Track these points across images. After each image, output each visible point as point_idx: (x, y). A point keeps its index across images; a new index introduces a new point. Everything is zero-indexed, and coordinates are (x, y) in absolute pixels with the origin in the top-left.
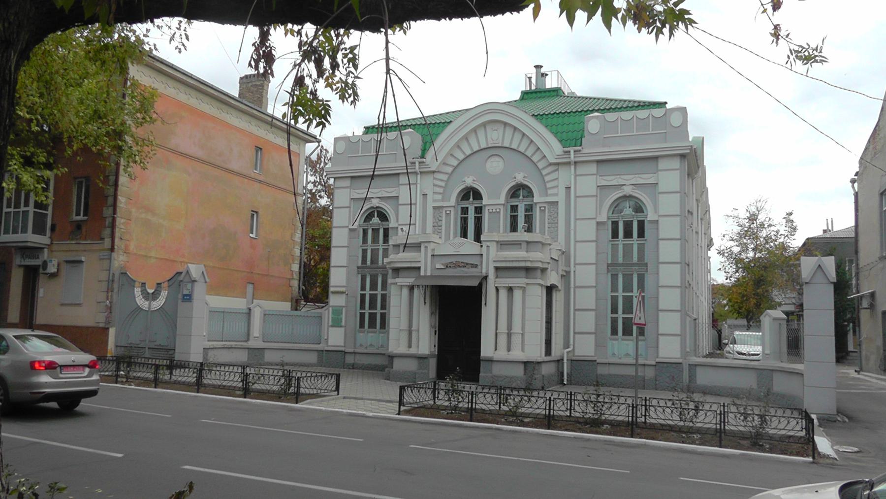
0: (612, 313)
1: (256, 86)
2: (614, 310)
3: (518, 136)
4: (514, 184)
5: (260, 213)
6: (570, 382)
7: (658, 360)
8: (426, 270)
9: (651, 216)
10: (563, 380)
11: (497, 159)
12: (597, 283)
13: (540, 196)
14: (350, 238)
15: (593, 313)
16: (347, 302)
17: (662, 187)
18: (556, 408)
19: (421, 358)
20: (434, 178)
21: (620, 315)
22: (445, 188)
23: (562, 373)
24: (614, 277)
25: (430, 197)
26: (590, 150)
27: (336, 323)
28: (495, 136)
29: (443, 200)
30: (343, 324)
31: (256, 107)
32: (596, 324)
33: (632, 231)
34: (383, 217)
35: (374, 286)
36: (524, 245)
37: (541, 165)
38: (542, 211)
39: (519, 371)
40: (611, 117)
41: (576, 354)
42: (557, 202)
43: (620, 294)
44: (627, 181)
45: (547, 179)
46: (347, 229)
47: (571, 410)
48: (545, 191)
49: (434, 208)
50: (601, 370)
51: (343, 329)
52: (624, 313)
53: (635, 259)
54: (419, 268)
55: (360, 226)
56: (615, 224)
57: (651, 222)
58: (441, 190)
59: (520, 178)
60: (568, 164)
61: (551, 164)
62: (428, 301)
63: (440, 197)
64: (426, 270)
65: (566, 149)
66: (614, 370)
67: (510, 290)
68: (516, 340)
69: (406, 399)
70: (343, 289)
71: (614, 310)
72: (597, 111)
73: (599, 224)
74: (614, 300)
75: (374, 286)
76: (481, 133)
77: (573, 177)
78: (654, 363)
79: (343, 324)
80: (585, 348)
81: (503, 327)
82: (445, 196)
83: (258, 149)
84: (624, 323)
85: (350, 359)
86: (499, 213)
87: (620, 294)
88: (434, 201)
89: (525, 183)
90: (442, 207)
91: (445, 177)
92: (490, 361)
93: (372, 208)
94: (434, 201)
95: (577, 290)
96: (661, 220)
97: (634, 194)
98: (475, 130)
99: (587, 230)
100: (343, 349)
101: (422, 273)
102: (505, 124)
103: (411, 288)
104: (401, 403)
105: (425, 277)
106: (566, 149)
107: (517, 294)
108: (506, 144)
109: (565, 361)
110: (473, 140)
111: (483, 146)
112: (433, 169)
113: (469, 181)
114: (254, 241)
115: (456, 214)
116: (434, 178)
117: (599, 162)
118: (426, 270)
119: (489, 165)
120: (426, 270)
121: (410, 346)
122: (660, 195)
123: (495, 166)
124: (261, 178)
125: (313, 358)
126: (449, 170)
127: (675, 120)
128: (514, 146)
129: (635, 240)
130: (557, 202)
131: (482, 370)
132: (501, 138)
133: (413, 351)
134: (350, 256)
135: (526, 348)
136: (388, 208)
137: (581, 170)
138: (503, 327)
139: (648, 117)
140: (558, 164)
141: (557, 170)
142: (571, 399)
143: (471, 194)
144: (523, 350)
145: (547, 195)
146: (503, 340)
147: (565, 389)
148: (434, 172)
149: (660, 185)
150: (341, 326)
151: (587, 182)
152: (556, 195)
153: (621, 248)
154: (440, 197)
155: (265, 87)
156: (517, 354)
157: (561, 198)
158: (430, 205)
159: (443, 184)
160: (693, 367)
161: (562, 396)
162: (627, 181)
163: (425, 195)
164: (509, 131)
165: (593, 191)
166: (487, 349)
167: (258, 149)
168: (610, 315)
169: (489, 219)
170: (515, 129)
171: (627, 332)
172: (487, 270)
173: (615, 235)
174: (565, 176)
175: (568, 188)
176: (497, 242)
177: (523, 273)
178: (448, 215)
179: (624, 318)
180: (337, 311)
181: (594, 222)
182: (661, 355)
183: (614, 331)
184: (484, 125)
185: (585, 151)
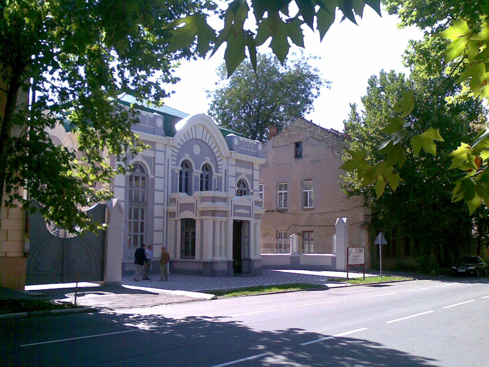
19: (228, 262)
34: (143, 170)
35: (136, 217)
42: (221, 177)
45: (219, 163)
59: (208, 160)
63: (175, 163)
75: (136, 217)
88: (173, 165)
93: (137, 161)
94: (173, 165)
103: (221, 222)
113: (187, 156)
116: (172, 151)
117: (236, 160)
133: (224, 258)
145: (218, 172)
152: (221, 173)
158: (171, 167)
159: (176, 155)
163: (168, 160)
165: (234, 175)
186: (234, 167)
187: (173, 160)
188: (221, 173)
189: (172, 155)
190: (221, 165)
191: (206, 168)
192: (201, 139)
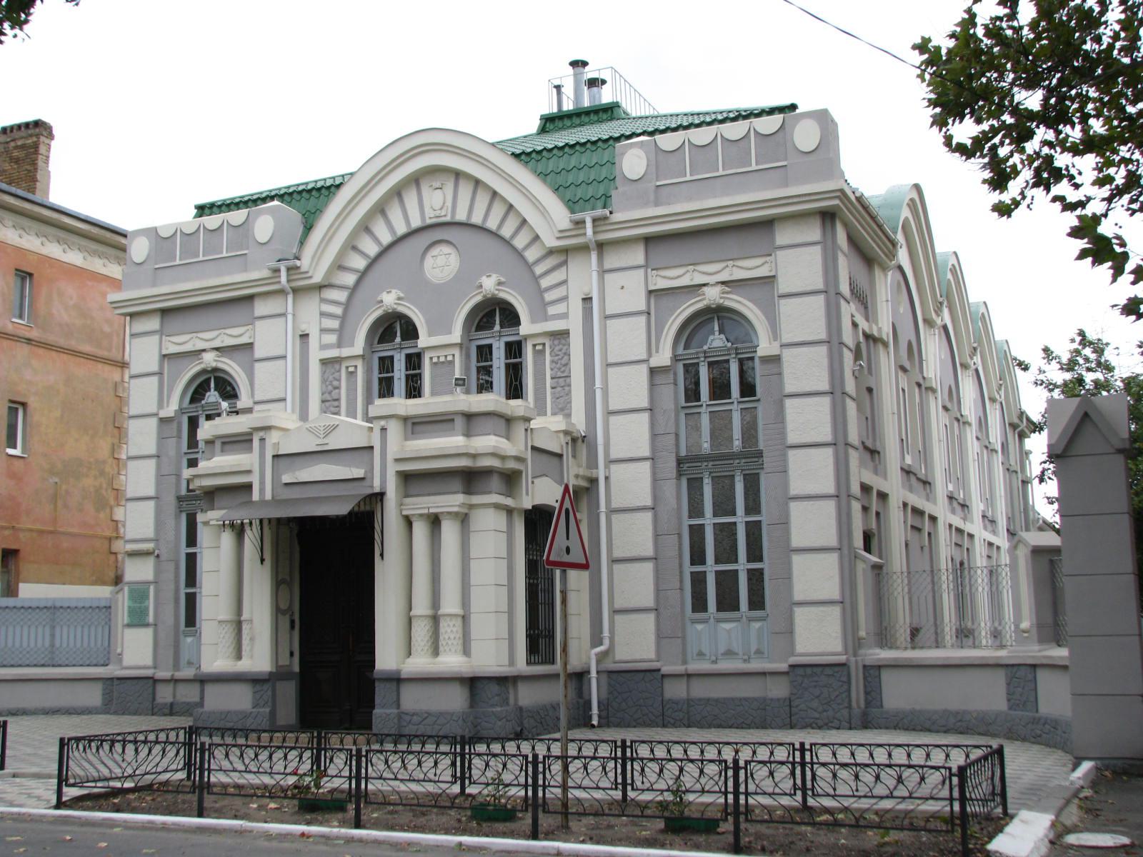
0: (761, 572)
1: (23, 147)
2: (698, 556)
3: (482, 200)
4: (479, 298)
5: (33, 402)
6: (605, 722)
7: (793, 660)
8: (262, 490)
9: (765, 346)
10: (590, 718)
11: (445, 249)
12: (655, 497)
13: (534, 321)
14: (161, 438)
15: (649, 566)
16: (158, 571)
17: (783, 286)
18: (752, 788)
19: (255, 680)
20: (323, 300)
21: (711, 568)
22: (343, 318)
23: (589, 703)
24: (695, 486)
25: (313, 342)
26: (629, 214)
27: (138, 619)
28: (436, 202)
29: (339, 345)
30: (151, 619)
31: (20, 192)
32: (658, 591)
33: (728, 385)
36: (459, 422)
37: (531, 255)
38: (539, 354)
39: (456, 700)
40: (668, 142)
41: (618, 657)
42: (565, 334)
43: (709, 520)
44: (710, 277)
46: (153, 422)
47: (463, 779)
48: (541, 311)
49: (324, 362)
50: (675, 691)
51: (149, 632)
52: (717, 561)
53: (737, 444)
54: (248, 487)
55: (181, 411)
56: (691, 371)
57: (767, 360)
58: (335, 324)
59: (489, 284)
60: (584, 249)
61: (551, 252)
62: (267, 556)
63: (332, 338)
64: (263, 490)
65: (578, 216)
66: (701, 690)
67: (435, 521)
68: (450, 630)
69: (75, 769)
70: (150, 546)
71: (698, 556)
72: (643, 133)
73: (653, 372)
74: (697, 533)
76: (411, 199)
77: (595, 275)
78: (783, 667)
79: (151, 619)
80: (636, 643)
81: (421, 606)
82: (343, 337)
83: (24, 276)
84: (718, 584)
85: (164, 695)
86: (452, 363)
87: (709, 520)
88: (323, 347)
89: (503, 295)
90: (338, 360)
91: (341, 296)
92: (396, 680)
93: (204, 371)
94: (323, 347)
95: (614, 517)
96: (787, 355)
97: (728, 303)
98: (397, 193)
99: (631, 387)
100: (149, 673)
101: (256, 496)
102: (458, 175)
104: (62, 780)
105: (263, 502)
106: (578, 216)
107: (449, 531)
108: (461, 216)
109: (594, 674)
110: (395, 214)
111: (416, 223)
112: (318, 278)
113: (390, 300)
114: (17, 463)
115: (368, 371)
117: (648, 240)
118: (263, 490)
119: (429, 262)
120: (262, 490)
121: (239, 656)
122: (783, 301)
123: (442, 264)
124: (34, 334)
125: (93, 696)
126: (350, 279)
127: (805, 136)
128: (477, 219)
129: (735, 404)
130: (565, 334)
131: (378, 700)
132: (449, 204)
134: (160, 476)
135: (475, 646)
136: (232, 367)
137: (612, 260)
138: (421, 606)
139: (747, 136)
140: (565, 251)
141: (565, 263)
142: (624, 758)
143: (394, 328)
144: (466, 651)
145: (546, 318)
146: (421, 632)
147: (590, 734)
148: (320, 287)
149: (780, 280)
150: (147, 625)
151: (627, 287)
152: (564, 316)
153: (705, 421)
154: (332, 338)
155: (42, 149)
156: (451, 661)
157: (574, 324)
158: (315, 355)
160: (873, 672)
161: (604, 750)
162: (710, 277)
163: (304, 336)
164: (465, 191)
166: (387, 657)
167: (24, 276)
168: (688, 569)
169: (433, 378)
170: (477, 182)
171: (728, 602)
172: (383, 481)
173: (693, 394)
174: (582, 276)
175: (587, 300)
176: (405, 419)
177: (457, 484)
178: (352, 374)
179: (717, 573)
180: (139, 594)
181: (643, 370)
182: (800, 648)
183: (699, 604)
184: (415, 180)
185: (618, 217)
186: (642, 271)
187: (323, 331)
188: (564, 316)
189: (323, 314)
190: (565, 282)
191: (496, 313)
192: (448, 219)
